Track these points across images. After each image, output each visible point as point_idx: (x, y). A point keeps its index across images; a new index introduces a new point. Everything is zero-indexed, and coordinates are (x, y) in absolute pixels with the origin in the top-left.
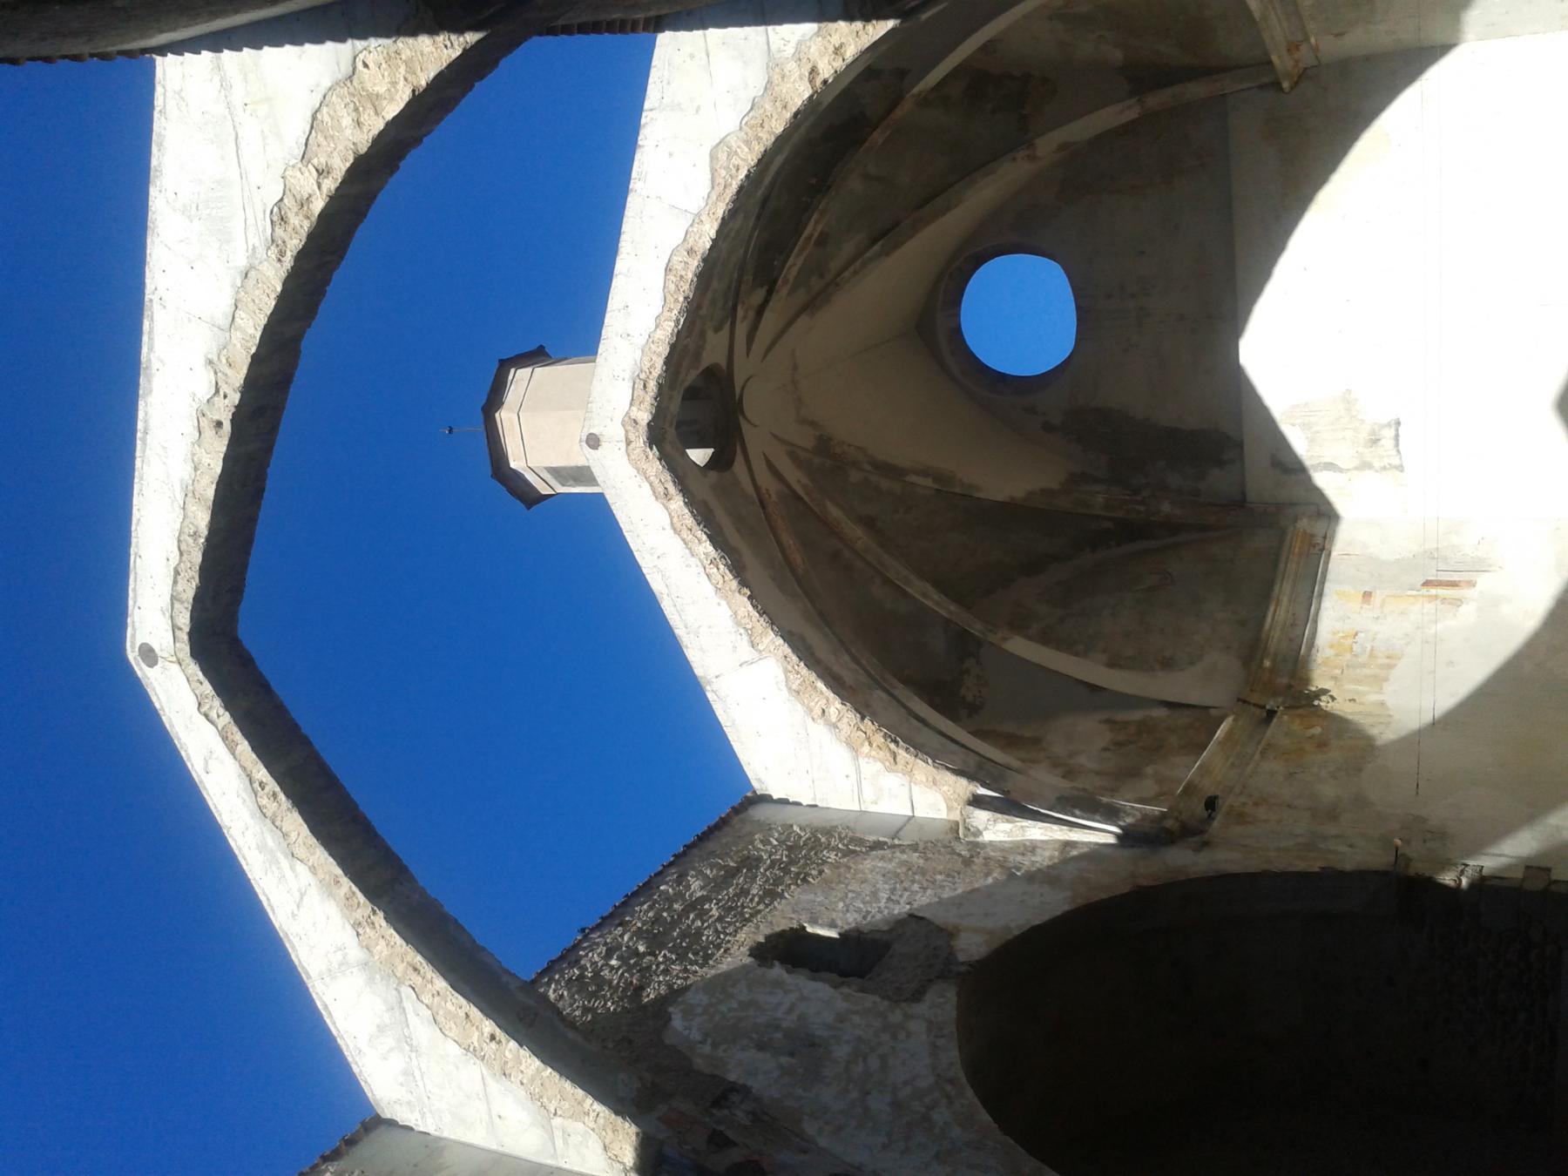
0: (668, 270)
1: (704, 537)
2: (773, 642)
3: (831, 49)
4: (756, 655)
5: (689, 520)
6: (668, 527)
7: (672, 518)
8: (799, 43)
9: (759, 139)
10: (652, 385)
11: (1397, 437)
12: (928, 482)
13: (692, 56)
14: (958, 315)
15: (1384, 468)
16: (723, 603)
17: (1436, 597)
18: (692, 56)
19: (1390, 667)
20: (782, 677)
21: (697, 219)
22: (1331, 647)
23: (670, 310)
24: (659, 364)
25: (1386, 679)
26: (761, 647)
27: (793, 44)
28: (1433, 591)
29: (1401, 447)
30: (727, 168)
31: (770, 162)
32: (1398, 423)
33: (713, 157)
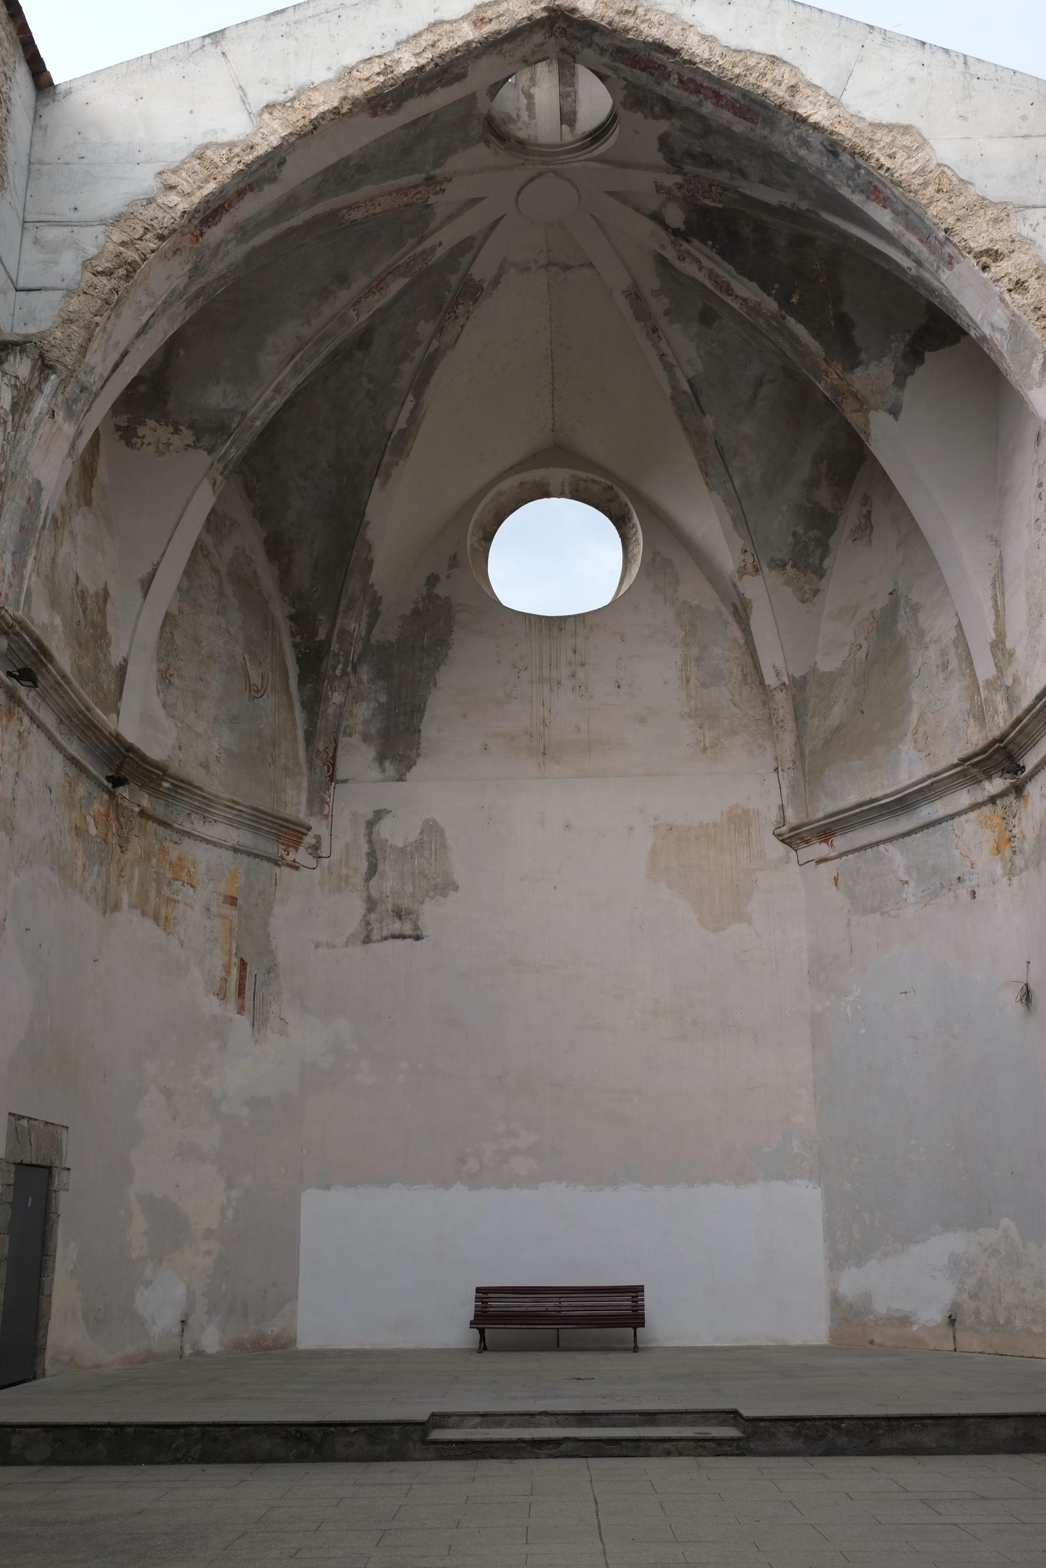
0: (774, 60)
1: (422, 61)
2: (275, 132)
3: (1023, 277)
4: (256, 108)
5: (445, 45)
6: (437, 16)
7: (451, 22)
8: (1032, 242)
9: (925, 185)
10: (629, 21)
11: (403, 937)
12: (402, 424)
13: (1024, 118)
14: (561, 495)
15: (368, 923)
16: (330, 75)
17: (228, 973)
18: (1024, 118)
19: (156, 919)
20: (224, 138)
21: (833, 102)
22: (180, 859)
23: (722, 56)
24: (656, 33)
25: (144, 914)
26: (266, 116)
27: (1032, 235)
28: (235, 971)
29: (391, 940)
30: (891, 144)
31: (885, 202)
32: (418, 938)
33: (906, 129)
